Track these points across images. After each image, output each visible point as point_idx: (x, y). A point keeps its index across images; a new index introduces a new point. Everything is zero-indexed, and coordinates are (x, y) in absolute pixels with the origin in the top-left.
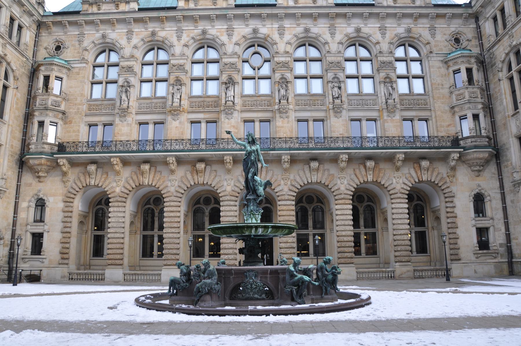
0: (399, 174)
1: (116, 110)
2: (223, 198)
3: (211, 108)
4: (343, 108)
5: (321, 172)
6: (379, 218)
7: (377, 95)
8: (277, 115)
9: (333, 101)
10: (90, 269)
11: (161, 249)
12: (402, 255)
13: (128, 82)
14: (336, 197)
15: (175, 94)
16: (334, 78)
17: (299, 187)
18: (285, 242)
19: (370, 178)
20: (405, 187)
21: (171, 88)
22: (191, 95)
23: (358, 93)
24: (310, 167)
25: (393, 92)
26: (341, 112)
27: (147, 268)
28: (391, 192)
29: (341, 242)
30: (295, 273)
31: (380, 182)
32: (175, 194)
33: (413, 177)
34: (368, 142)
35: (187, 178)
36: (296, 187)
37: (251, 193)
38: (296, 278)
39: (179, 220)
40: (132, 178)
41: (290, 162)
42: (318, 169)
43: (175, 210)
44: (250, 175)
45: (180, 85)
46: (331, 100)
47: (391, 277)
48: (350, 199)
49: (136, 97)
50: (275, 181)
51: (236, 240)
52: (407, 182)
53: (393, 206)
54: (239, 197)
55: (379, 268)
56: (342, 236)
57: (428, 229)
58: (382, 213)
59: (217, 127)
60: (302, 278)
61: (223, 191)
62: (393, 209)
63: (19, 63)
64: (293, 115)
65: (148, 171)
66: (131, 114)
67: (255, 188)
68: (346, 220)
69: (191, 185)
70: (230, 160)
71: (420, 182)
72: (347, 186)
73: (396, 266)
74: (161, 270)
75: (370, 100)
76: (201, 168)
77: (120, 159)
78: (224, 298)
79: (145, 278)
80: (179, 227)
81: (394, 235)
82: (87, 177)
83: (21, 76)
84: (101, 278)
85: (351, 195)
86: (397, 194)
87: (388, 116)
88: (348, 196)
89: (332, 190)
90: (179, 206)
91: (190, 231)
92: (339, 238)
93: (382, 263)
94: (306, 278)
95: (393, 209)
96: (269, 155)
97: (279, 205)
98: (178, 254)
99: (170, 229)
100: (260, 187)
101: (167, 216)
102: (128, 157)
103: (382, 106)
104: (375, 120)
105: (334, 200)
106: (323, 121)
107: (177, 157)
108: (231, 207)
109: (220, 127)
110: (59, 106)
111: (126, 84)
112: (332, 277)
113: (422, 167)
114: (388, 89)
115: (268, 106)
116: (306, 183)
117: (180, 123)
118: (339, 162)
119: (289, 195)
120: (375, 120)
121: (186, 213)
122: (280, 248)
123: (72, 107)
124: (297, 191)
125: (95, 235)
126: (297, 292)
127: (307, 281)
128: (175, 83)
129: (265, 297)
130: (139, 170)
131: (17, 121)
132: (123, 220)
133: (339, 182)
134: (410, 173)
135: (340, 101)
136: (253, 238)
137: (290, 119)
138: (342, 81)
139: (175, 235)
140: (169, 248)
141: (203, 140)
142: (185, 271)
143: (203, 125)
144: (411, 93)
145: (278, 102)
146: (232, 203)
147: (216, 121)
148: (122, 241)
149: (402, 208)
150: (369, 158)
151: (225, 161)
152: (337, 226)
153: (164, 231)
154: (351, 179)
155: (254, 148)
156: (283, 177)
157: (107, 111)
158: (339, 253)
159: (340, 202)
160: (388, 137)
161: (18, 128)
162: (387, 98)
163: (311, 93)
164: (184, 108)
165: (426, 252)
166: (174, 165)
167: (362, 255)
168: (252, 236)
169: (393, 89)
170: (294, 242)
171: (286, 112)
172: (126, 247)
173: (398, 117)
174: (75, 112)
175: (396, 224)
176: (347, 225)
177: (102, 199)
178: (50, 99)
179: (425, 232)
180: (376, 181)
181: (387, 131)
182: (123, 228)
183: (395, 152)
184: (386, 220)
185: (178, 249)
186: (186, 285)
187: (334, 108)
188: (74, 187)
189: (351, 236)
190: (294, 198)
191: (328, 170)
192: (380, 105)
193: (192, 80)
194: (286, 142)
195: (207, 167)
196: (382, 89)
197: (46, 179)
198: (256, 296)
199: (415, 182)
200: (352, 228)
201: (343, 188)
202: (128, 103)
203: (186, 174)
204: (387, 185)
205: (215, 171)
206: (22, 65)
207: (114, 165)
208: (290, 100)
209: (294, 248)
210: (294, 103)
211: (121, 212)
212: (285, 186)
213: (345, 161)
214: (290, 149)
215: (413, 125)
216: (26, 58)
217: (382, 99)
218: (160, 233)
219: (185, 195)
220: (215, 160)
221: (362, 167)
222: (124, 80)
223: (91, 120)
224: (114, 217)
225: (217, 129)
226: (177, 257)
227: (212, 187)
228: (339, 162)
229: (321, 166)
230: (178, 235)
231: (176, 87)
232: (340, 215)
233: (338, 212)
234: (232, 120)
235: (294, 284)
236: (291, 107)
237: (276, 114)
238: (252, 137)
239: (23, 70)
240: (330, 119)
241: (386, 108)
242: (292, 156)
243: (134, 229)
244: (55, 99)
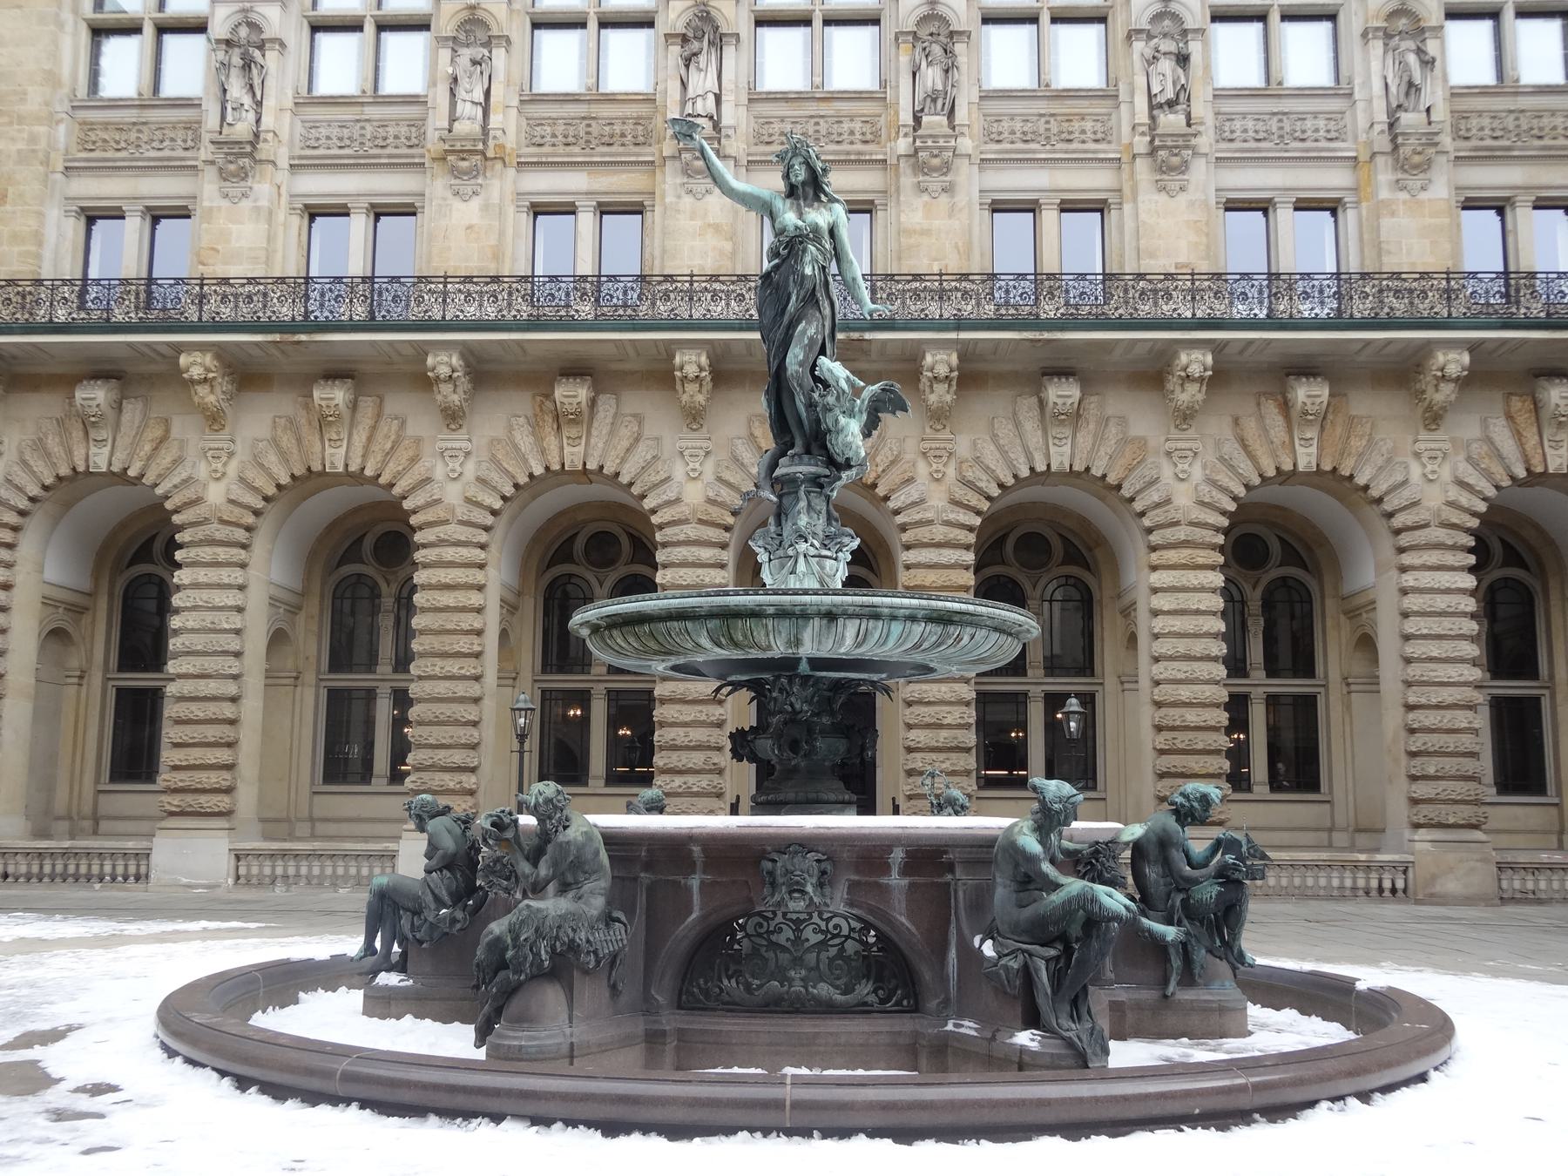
0: (1437, 440)
1: (202, 149)
2: (668, 531)
3: (621, 149)
4: (1193, 148)
5: (1092, 426)
6: (1332, 635)
7: (1351, 95)
8: (903, 179)
9: (1153, 118)
10: (95, 833)
11: (400, 749)
12: (1442, 797)
13: (254, 27)
14: (1155, 538)
15: (464, 83)
16: (1157, 18)
17: (995, 492)
18: (928, 726)
19: (1306, 458)
20: (1465, 499)
21: (445, 54)
22: (535, 91)
23: (1263, 85)
24: (1042, 404)
25: (1424, 78)
26: (1183, 167)
27: (345, 828)
28: (1398, 521)
29: (1173, 729)
30: (1046, 867)
31: (1351, 477)
32: (462, 512)
33: (1501, 457)
34: (1306, 295)
35: (516, 447)
36: (980, 491)
37: (798, 449)
38: (1056, 898)
39: (477, 625)
40: (275, 442)
41: (959, 377)
42: (1078, 415)
43: (462, 580)
44: (795, 356)
45: (483, 45)
46: (1142, 116)
47: (1394, 890)
48: (1213, 547)
49: (290, 93)
50: (893, 463)
51: (718, 690)
52: (1473, 478)
53: (1409, 580)
54: (736, 531)
55: (1330, 846)
56: (1174, 705)
57: (1551, 688)
58: (1346, 613)
59: (647, 232)
60: (1086, 902)
61: (669, 503)
62: (1404, 592)
64: (971, 183)
65: (346, 413)
66: (270, 166)
67: (818, 421)
68: (1196, 636)
69: (531, 476)
70: (701, 369)
71: (1535, 478)
72: (1205, 488)
73: (1418, 846)
74: (397, 838)
75: (1315, 115)
76: (575, 401)
77: (218, 357)
78: (647, 997)
79: (329, 871)
80: (478, 655)
81: (1410, 708)
82: (77, 434)
84: (132, 869)
85: (1217, 530)
86: (1427, 530)
87: (1399, 185)
88: (1204, 532)
89: (1138, 506)
90: (481, 566)
91: (527, 675)
92: (1164, 711)
93: (1344, 830)
94: (1115, 900)
95: (1404, 592)
96: (866, 353)
97: (908, 567)
98: (473, 770)
99: (439, 662)
100: (843, 420)
101: (427, 605)
102: (256, 352)
103: (1369, 143)
104: (1333, 207)
105: (1143, 550)
106: (1101, 211)
107: (472, 352)
108: (700, 571)
109: (658, 229)
111: (243, 32)
112: (1220, 894)
113: (1545, 415)
114: (1403, 65)
115: (866, 142)
116: (1024, 472)
117: (486, 208)
118: (1170, 386)
119: (948, 523)
120: (1333, 207)
121: (510, 597)
122: (910, 750)
124: (985, 506)
125: (119, 690)
126: (1057, 979)
127: (1117, 918)
128: (462, 36)
129: (872, 998)
130: (308, 406)
132: (236, 621)
133: (1167, 472)
134: (1489, 441)
135: (1182, 118)
136: (805, 679)
137: (961, 199)
138: (1196, 31)
139: (461, 689)
140: (432, 741)
141: (584, 278)
142: (448, 844)
143: (586, 220)
144: (1508, 82)
145: (911, 122)
146: (706, 554)
147: (641, 204)
148: (228, 710)
149: (1448, 591)
150: (1304, 367)
151: (678, 374)
152: (1157, 660)
153: (414, 669)
154: (1222, 459)
155: (819, 217)
156: (927, 445)
157: (166, 153)
158: (1162, 776)
159: (1172, 556)
160: (1396, 275)
162: (1394, 105)
163: (1053, 87)
164: (502, 147)
165: (1541, 789)
166: (460, 390)
167: (1255, 788)
168: (804, 668)
169: (1428, 63)
170: (967, 726)
171: (946, 168)
172: (249, 737)
173: (1441, 187)
174: (19, 151)
175: (1420, 660)
176: (1201, 659)
177: (153, 538)
179: (1535, 701)
180: (1335, 469)
181: (1389, 252)
182: (238, 655)
183: (1429, 342)
184: (1367, 643)
185: (474, 747)
186: (454, 921)
187: (1153, 152)
188: (17, 481)
189: (1217, 706)
190: (971, 538)
191: (1123, 421)
192: (1363, 137)
193: (536, 25)
194: (942, 295)
195: (602, 398)
196: (1376, 66)
198: (824, 990)
199: (1513, 478)
200: (1220, 671)
201: (1183, 499)
202: (258, 121)
203: (510, 429)
204: (1384, 487)
205: (634, 415)
207: (193, 381)
208: (961, 115)
209: (968, 750)
210: (977, 128)
211: (229, 586)
212: (934, 486)
213: (1201, 379)
214: (960, 324)
215: (1509, 226)
217: (1370, 109)
218: (399, 681)
219: (505, 517)
220: (633, 373)
221: (1271, 409)
222: (239, 17)
224: (195, 608)
225: (647, 242)
226: (469, 781)
227: (621, 485)
228: (1172, 383)
229: (1093, 402)
230: (474, 689)
231: (466, 54)
232: (1169, 613)
233: (1163, 602)
234: (709, 198)
235: (1044, 931)
236: (966, 144)
237: (898, 176)
238: (808, 164)
240: (1135, 200)
241: (1388, 147)
242: (967, 353)
243: (290, 664)
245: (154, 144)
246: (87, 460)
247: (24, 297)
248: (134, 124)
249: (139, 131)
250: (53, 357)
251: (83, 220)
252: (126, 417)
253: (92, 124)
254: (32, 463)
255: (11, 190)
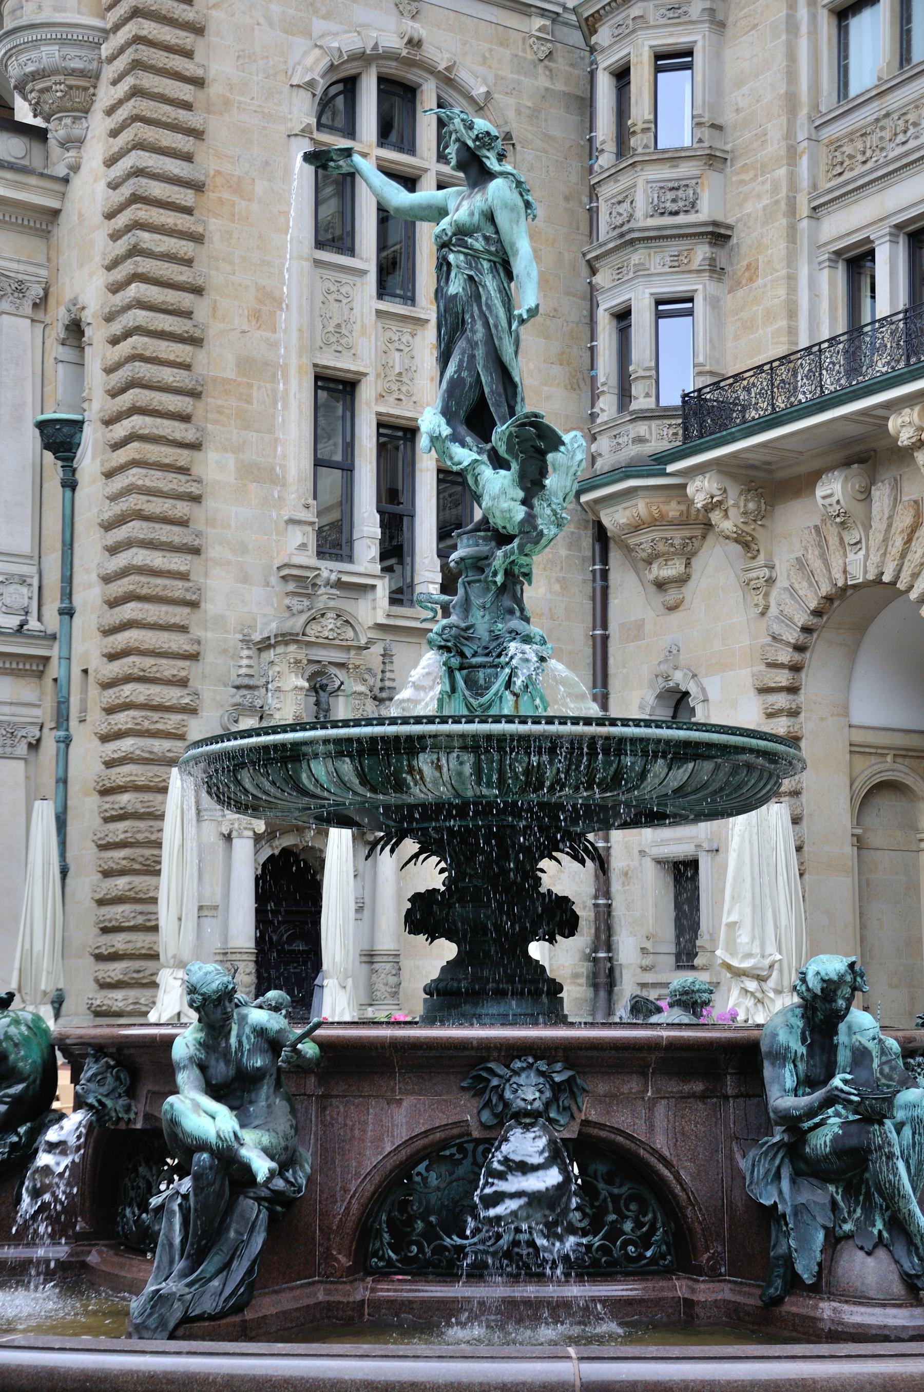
63: (508, 53)
82: (833, 541)
83: (534, 115)
110: (693, 205)
123: (750, 186)
131: (547, 337)
161: (557, 370)
178: (640, 183)
197: (688, 589)
206: (529, 56)
216: (543, 12)
223: (844, 228)
239: (543, 81)
244: (665, 173)
245: (898, 141)
246: (845, 572)
247: (749, 392)
248: (877, 120)
249: (883, 128)
250: (801, 453)
251: (841, 268)
252: (876, 507)
253: (839, 140)
254: (796, 586)
255: (761, 258)
